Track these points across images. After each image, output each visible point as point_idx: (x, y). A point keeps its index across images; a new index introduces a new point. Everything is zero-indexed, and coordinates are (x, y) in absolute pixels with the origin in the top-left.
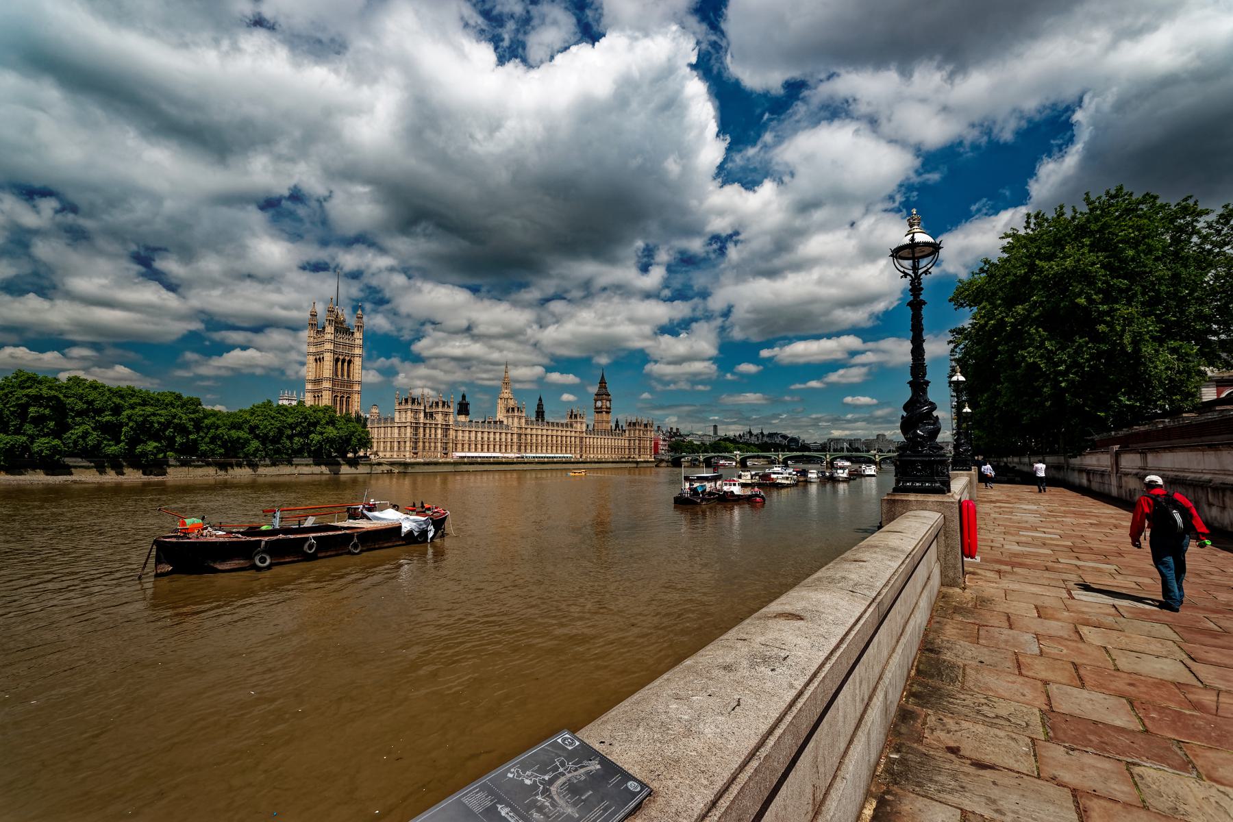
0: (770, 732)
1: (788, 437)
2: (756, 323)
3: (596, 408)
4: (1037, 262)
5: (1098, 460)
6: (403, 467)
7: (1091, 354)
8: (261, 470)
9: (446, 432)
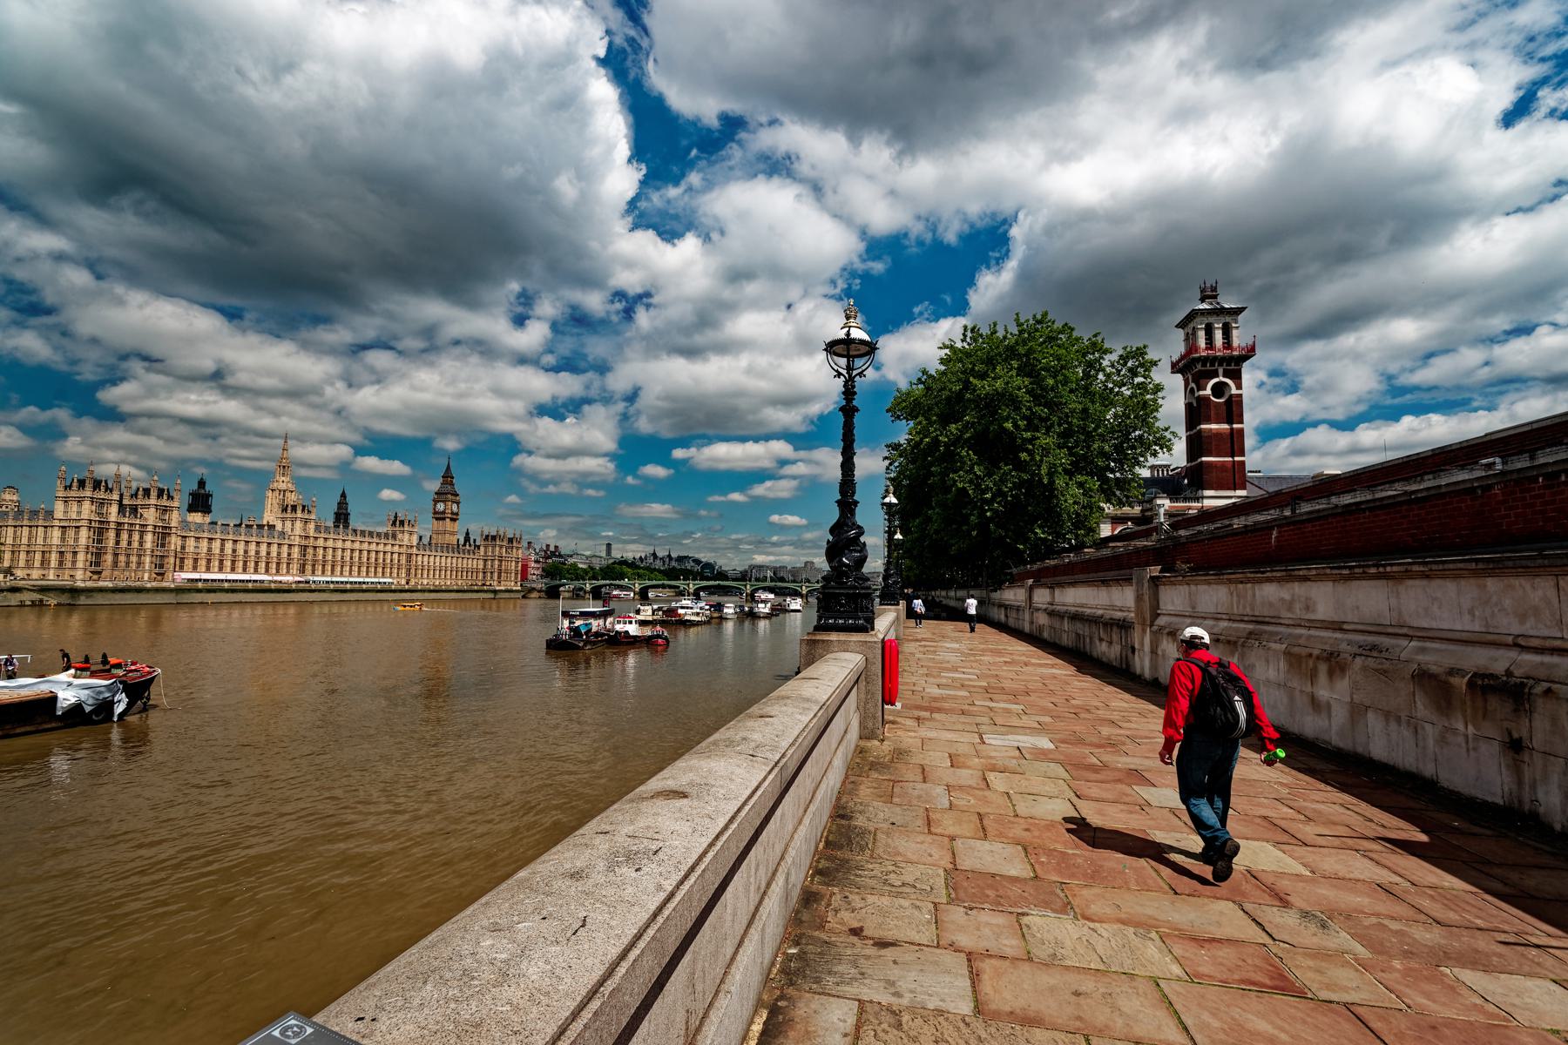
0: (623, 956)
1: (701, 562)
2: (671, 413)
3: (435, 513)
4: (971, 379)
5: (1015, 595)
6: (67, 595)
7: (1014, 483)
9: (164, 538)
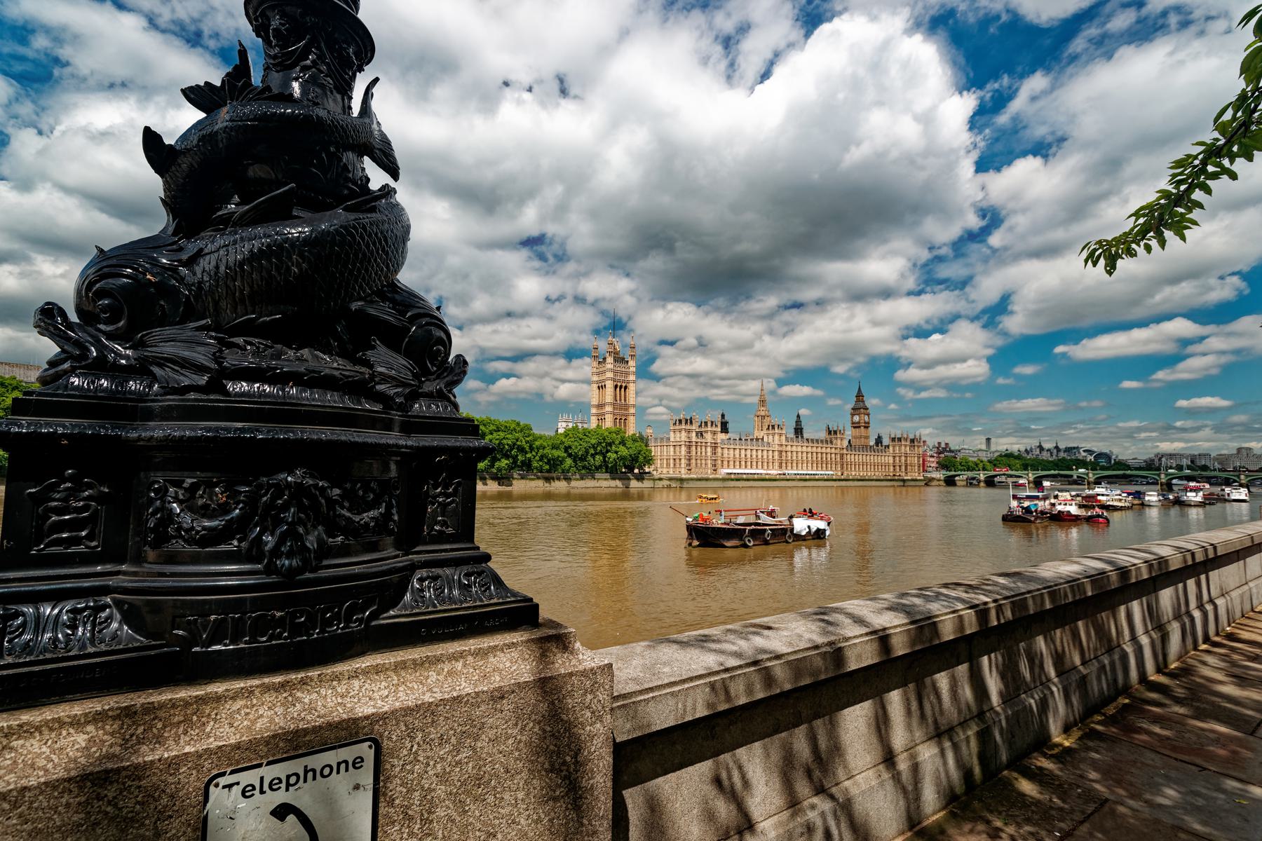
1: (1094, 452)
6: (679, 482)
8: (573, 483)
